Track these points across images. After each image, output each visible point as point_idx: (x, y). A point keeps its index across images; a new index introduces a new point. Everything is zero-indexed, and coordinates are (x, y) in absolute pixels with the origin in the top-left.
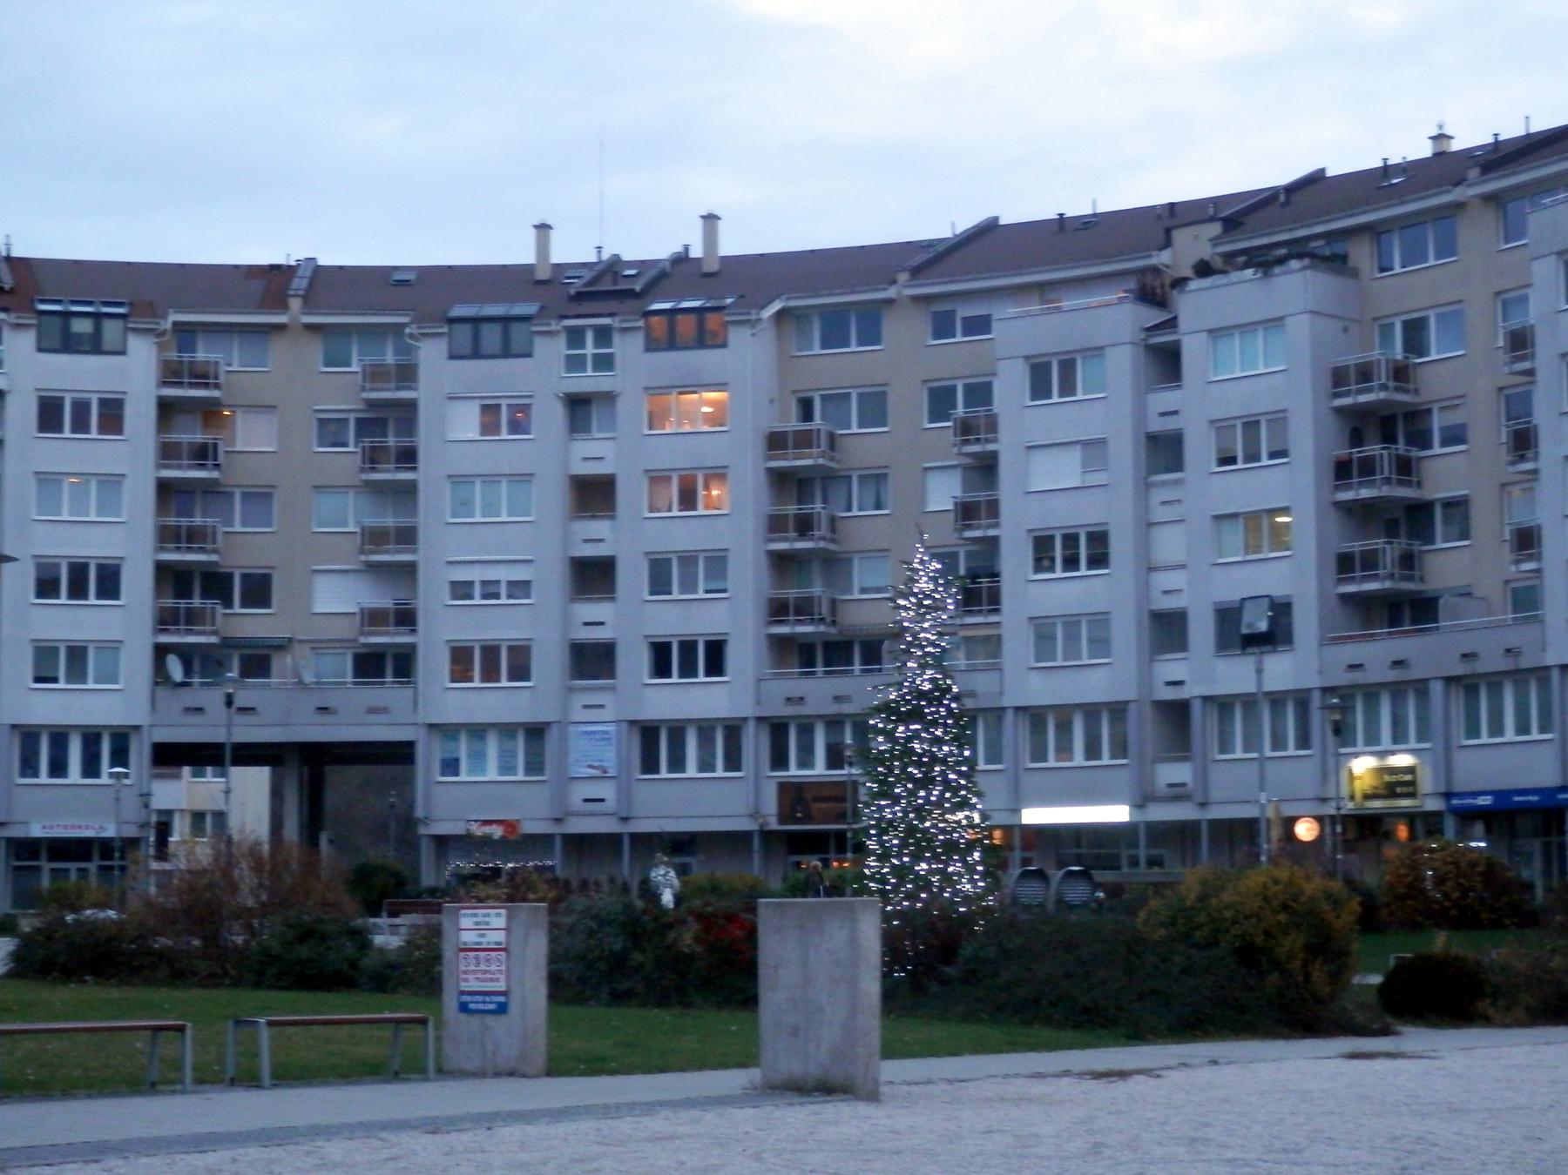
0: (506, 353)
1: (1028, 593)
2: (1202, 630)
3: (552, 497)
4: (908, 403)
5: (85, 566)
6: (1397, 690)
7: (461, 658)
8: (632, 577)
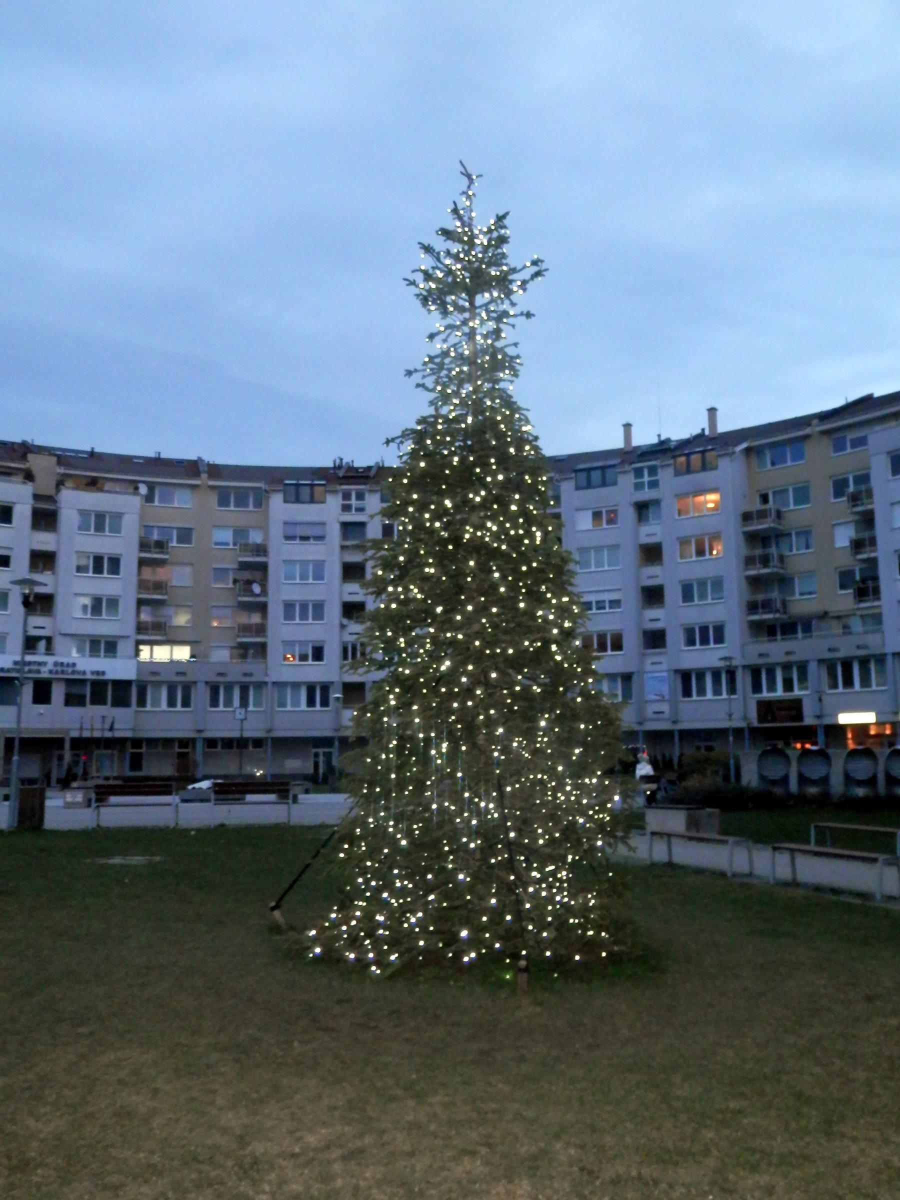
0: (604, 484)
3: (629, 555)
4: (822, 491)
7: (289, 607)
8: (673, 594)
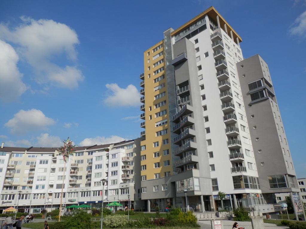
1: (35, 183)
2: (55, 186)
5: (62, 171)
6: (74, 193)
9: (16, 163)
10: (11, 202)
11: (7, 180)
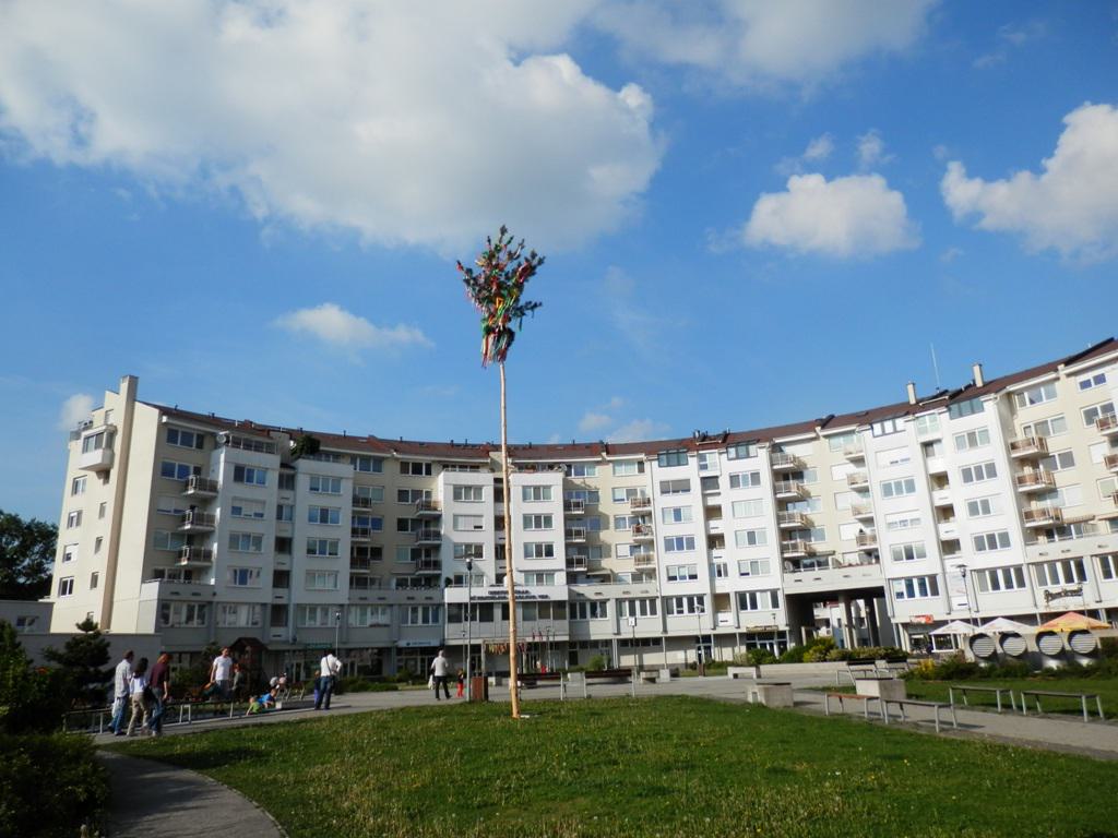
0: (895, 431)
8: (961, 510)
9: (1042, 426)
10: (1078, 593)
11: (1035, 505)
